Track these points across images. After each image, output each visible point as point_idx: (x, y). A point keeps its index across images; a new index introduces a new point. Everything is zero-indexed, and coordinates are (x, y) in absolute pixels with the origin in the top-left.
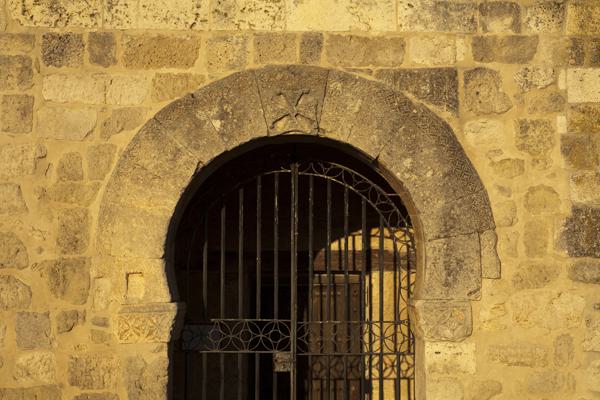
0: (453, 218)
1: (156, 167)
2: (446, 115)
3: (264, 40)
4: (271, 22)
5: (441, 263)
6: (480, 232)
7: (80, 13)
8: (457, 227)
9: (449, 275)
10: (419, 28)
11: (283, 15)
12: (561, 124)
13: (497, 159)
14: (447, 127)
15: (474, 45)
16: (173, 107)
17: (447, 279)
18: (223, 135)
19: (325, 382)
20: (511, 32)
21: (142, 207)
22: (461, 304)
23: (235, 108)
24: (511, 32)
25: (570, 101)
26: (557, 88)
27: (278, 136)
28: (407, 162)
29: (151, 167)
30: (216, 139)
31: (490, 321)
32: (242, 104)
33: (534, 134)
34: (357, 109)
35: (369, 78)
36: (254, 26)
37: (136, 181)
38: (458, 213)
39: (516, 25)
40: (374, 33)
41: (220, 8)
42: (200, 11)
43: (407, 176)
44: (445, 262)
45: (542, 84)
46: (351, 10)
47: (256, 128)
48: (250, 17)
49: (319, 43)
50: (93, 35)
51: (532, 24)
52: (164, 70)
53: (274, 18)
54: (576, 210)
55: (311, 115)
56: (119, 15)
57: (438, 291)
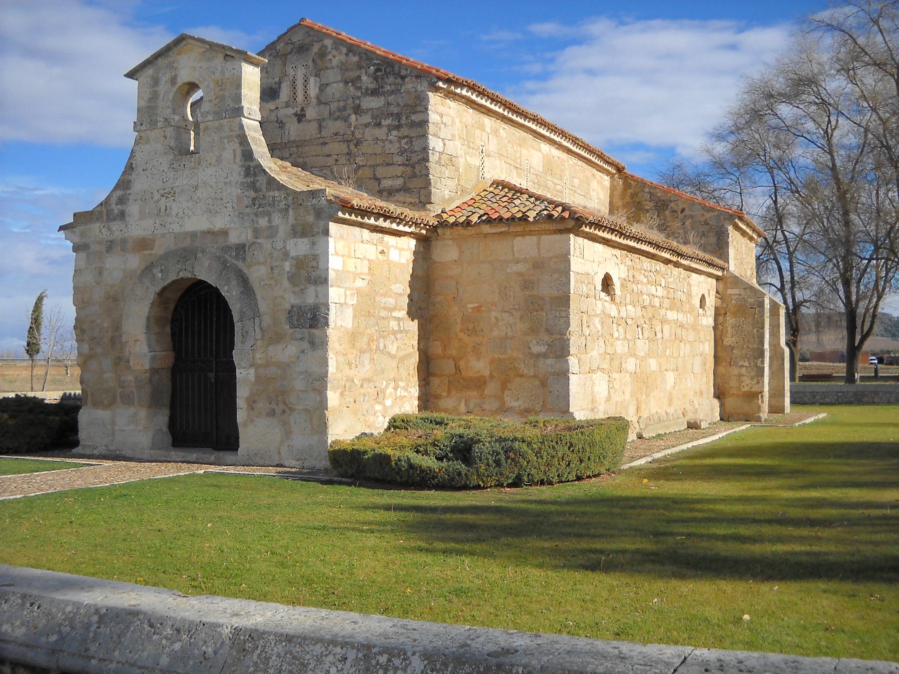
2: (240, 264)
3: (177, 236)
5: (240, 332)
10: (233, 225)
12: (287, 266)
13: (263, 284)
14: (240, 271)
15: (254, 232)
16: (146, 268)
18: (162, 279)
20: (268, 224)
23: (165, 268)
24: (268, 224)
25: (291, 255)
26: (286, 249)
28: (226, 288)
30: (162, 279)
33: (276, 271)
34: (207, 265)
35: (214, 250)
39: (270, 221)
40: (216, 229)
43: (226, 294)
45: (279, 248)
47: (173, 277)
48: (172, 226)
49: (197, 236)
50: (121, 239)
51: (276, 219)
52: (145, 252)
54: (292, 307)
57: (240, 345)
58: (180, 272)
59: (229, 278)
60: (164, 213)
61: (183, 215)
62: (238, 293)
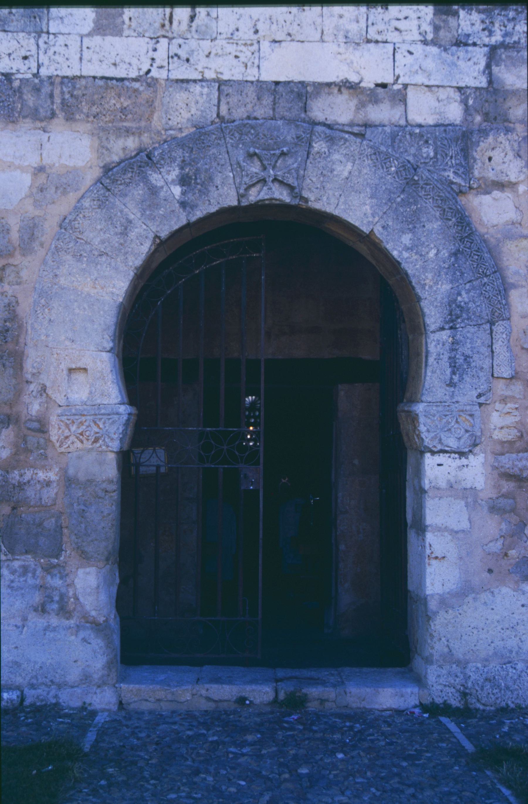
0: (459, 306)
1: (103, 242)
4: (243, 69)
5: (445, 357)
6: (492, 323)
7: (9, 55)
8: (464, 315)
9: (453, 373)
11: (256, 62)
17: (451, 379)
18: (183, 204)
19: (454, 194)
21: (86, 289)
22: (468, 408)
27: (251, 205)
29: (96, 241)
31: (502, 428)
32: (207, 167)
34: (346, 174)
36: (221, 73)
37: (78, 257)
38: (466, 300)
41: (180, 52)
42: (156, 55)
43: (405, 255)
44: (450, 358)
46: (339, 56)
53: (246, 66)
55: (291, 181)
56: (57, 57)
58: (253, 185)
59: (416, 213)
60: (184, 26)
61: (255, 37)
62: (445, 253)
